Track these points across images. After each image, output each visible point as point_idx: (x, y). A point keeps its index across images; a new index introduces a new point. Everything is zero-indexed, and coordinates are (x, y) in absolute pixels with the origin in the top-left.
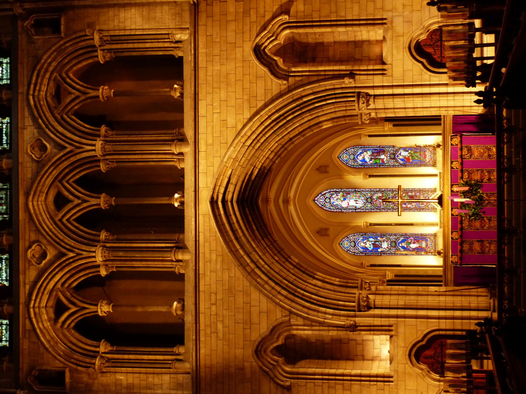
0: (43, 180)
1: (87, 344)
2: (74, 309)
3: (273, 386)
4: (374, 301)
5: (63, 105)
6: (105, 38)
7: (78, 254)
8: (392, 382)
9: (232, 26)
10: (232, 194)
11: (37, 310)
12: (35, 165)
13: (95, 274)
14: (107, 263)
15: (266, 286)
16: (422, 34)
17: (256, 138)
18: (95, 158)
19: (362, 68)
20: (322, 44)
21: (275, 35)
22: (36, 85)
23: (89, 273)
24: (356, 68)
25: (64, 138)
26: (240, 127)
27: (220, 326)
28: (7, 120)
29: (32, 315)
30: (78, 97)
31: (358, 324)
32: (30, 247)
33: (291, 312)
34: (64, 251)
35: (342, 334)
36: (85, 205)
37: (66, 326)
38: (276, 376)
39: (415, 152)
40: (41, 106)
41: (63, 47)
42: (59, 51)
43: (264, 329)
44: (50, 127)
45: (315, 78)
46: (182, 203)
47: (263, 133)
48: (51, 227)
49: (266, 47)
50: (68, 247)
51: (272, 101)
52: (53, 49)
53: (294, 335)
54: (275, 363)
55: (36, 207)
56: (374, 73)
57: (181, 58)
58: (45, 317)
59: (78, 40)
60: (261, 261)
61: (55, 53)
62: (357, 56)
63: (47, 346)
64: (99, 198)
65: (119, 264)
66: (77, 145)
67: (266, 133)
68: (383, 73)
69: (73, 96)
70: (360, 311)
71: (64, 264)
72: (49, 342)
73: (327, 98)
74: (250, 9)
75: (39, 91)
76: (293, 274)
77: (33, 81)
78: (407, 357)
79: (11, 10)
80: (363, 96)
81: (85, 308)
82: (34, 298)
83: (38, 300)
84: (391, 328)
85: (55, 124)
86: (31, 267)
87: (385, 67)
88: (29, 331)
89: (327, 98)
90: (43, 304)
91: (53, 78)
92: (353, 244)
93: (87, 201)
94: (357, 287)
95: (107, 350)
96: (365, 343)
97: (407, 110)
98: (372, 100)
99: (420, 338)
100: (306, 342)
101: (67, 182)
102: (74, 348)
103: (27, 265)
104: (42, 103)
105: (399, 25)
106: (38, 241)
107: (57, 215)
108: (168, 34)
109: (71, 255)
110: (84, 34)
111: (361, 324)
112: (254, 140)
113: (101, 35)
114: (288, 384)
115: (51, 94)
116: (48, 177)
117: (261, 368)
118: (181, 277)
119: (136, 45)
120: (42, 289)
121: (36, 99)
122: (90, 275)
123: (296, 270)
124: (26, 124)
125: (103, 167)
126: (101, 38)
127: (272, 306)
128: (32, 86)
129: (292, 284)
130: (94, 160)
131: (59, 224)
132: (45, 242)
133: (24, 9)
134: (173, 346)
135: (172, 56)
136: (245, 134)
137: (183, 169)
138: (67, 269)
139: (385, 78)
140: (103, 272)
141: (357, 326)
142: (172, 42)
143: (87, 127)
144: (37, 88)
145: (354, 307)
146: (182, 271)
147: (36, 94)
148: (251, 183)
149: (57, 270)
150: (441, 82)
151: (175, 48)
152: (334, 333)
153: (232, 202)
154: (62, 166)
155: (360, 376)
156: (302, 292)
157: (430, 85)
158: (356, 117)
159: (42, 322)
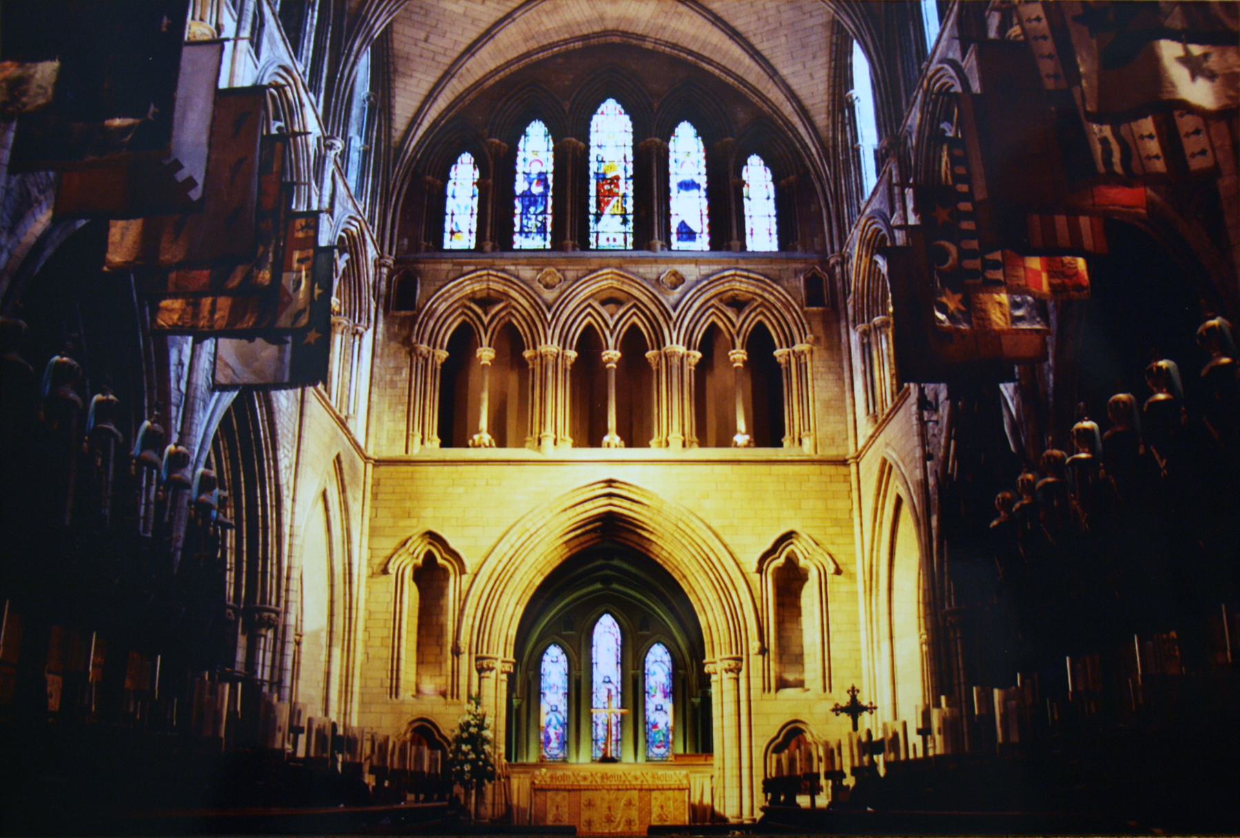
0: (637, 286)
2: (486, 320)
3: (389, 552)
4: (488, 677)
5: (724, 308)
6: (803, 357)
7: (549, 325)
8: (391, 697)
9: (820, 505)
11: (485, 278)
12: (654, 277)
13: (526, 345)
14: (539, 359)
15: (508, 546)
16: (812, 736)
17: (687, 534)
18: (662, 345)
19: (772, 664)
20: (799, 614)
21: (810, 557)
22: (748, 278)
24: (772, 656)
25: (686, 309)
26: (701, 515)
27: (461, 490)
28: (707, 248)
29: (479, 273)
30: (734, 326)
31: (461, 656)
32: (559, 270)
33: (476, 575)
34: (554, 309)
36: (607, 333)
37: (466, 311)
38: (400, 556)
39: (664, 735)
40: (723, 283)
41: (791, 309)
42: (787, 305)
44: (699, 293)
45: (759, 606)
46: (609, 446)
47: (693, 543)
48: (582, 294)
49: (796, 546)
50: (558, 313)
51: (731, 554)
52: (789, 298)
53: (447, 579)
54: (415, 555)
55: (605, 277)
56: (765, 677)
57: (781, 445)
58: (477, 287)
59: (800, 326)
60: (538, 539)
61: (784, 300)
62: (784, 657)
63: (443, 290)
64: (615, 349)
65: (538, 370)
66: (678, 324)
67: (693, 546)
68: (766, 688)
69: (734, 319)
70: (477, 659)
71: (537, 308)
72: (448, 291)
73: (736, 620)
74: (841, 527)
75: (740, 282)
76: (521, 579)
77: (751, 275)
78: (420, 716)
79: (833, 251)
80: (737, 665)
81: (486, 335)
82: (500, 274)
83: (497, 279)
84: (455, 697)
85: (701, 300)
86: (535, 272)
87: (773, 690)
88: (462, 270)
89: (736, 620)
90: (492, 285)
91: (755, 297)
92: (555, 659)
93: (611, 334)
94: (505, 656)
95: (436, 358)
96: (438, 665)
97: (720, 719)
98: (732, 675)
99: (442, 732)
100: (441, 593)
101: (635, 314)
102: (441, 321)
103: (538, 267)
104: (727, 285)
106: (565, 280)
107: (596, 299)
108: (809, 430)
109: (549, 317)
110: (808, 332)
111: (460, 661)
112: (684, 531)
113: (806, 352)
114: (390, 571)
115: (737, 295)
116: (640, 291)
117: (410, 538)
119: (795, 392)
120: (509, 284)
121: (731, 278)
122: (525, 339)
123: (527, 582)
124: (702, 267)
125: (650, 354)
126: (802, 352)
127: (484, 552)
128: (745, 274)
129: (511, 577)
130: (659, 342)
132: (565, 286)
133: (834, 267)
134: (439, 435)
135: (783, 435)
136: (691, 521)
137: (649, 446)
138: (532, 312)
139: (760, 691)
141: (458, 656)
142: (800, 434)
143: (698, 336)
144: (744, 280)
145: (482, 652)
146: (528, 444)
147: (737, 278)
148: (632, 528)
149: (532, 301)
150: (754, 760)
151: (794, 438)
153: (611, 505)
154: (652, 307)
155: (398, 659)
156: (500, 589)
157: (751, 747)
158: (711, 656)
159: (472, 284)
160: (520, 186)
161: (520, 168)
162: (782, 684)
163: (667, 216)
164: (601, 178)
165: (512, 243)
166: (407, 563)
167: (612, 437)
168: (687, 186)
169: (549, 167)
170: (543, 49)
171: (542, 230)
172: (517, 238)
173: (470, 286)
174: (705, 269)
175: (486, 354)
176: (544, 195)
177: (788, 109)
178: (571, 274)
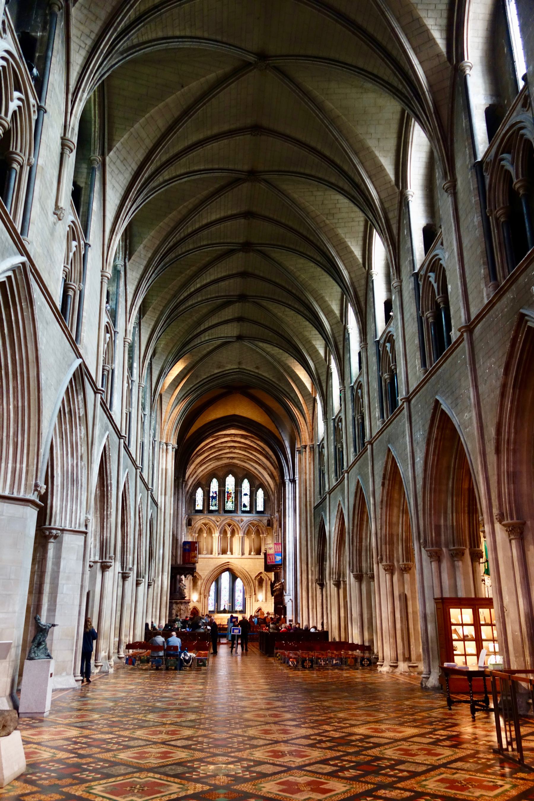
1: (197, 531)
10: (230, 567)
43: (200, 574)
57: (260, 554)
105: (265, 605)
118: (212, 554)
125: (236, 535)
131: (225, 525)
140: (213, 535)
143: (246, 532)
160: (211, 495)
161: (211, 490)
163: (241, 502)
164: (228, 492)
165: (209, 508)
167: (229, 553)
168: (246, 495)
169: (217, 490)
170: (217, 466)
171: (216, 505)
172: (211, 507)
173: (203, 521)
174: (248, 518)
176: (216, 497)
177: (266, 483)
178: (222, 519)
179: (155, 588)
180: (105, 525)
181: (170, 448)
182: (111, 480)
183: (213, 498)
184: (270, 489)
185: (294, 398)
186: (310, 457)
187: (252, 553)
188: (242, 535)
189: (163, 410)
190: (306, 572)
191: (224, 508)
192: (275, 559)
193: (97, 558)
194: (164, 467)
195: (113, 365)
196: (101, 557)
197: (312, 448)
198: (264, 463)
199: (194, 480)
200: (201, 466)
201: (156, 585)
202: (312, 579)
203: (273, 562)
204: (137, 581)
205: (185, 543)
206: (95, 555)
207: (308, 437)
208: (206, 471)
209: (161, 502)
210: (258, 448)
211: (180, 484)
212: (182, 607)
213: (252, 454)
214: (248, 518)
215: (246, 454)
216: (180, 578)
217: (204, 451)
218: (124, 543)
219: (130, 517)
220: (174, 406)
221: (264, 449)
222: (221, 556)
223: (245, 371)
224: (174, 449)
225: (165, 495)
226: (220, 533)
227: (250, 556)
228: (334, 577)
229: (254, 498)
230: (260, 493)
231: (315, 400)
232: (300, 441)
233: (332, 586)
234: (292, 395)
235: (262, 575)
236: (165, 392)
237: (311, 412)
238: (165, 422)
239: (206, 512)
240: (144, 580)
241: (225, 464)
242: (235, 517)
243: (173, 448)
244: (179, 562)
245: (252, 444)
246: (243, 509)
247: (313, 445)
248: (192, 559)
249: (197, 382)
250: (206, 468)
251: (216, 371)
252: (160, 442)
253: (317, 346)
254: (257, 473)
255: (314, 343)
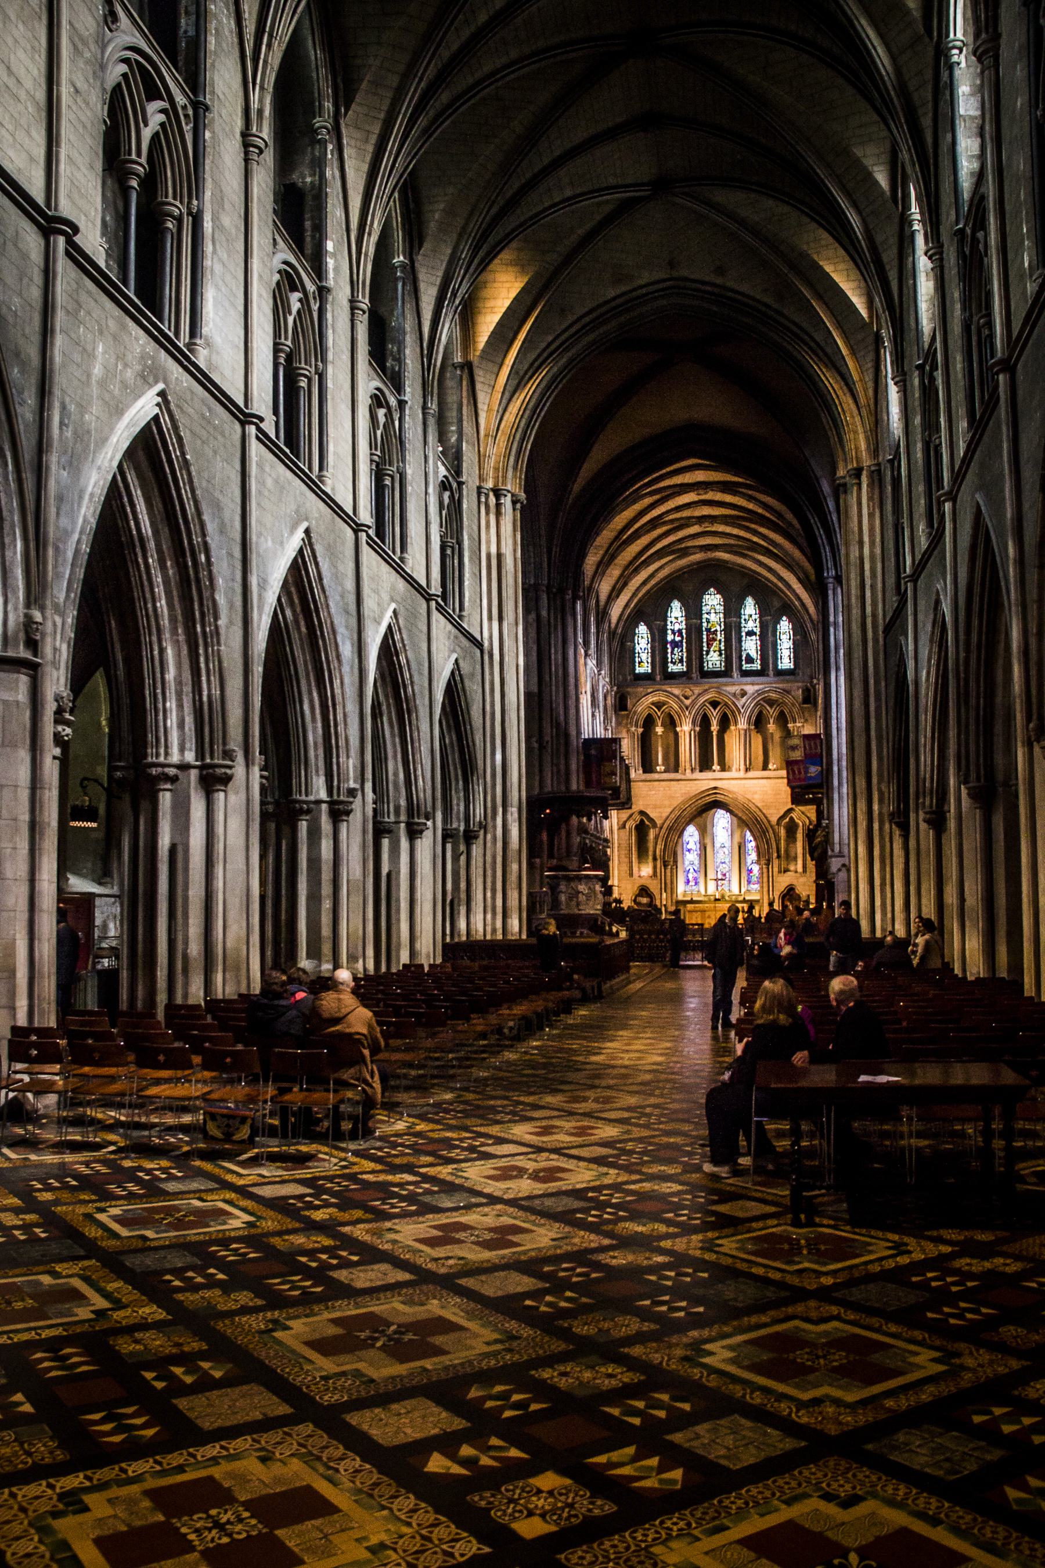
1: (641, 722)
10: (719, 798)
23: (678, 721)
35: (651, 853)
43: (652, 815)
100: (646, 834)
105: (802, 880)
125: (732, 728)
130: (736, 724)
131: (703, 704)
143: (753, 718)
152: (651, 849)
160: (670, 638)
162: (786, 871)
164: (708, 630)
166: (632, 824)
167: (716, 767)
168: (750, 633)
171: (681, 661)
173: (652, 699)
174: (757, 687)
175: (659, 730)
178: (696, 692)
179: (489, 845)
180: (203, 665)
181: (507, 501)
182: (204, 535)
183: (675, 644)
184: (806, 617)
185: (823, 344)
186: (870, 499)
187: (770, 766)
188: (745, 727)
189: (480, 406)
190: (864, 796)
191: (701, 666)
192: (806, 772)
193: (190, 757)
194: (494, 550)
195: (195, 202)
196: (200, 754)
197: (877, 477)
198: (786, 553)
199: (627, 606)
200: (637, 571)
201: (489, 837)
202: (880, 814)
203: (800, 780)
204: (409, 825)
205: (589, 743)
206: (182, 750)
207: (863, 446)
208: (653, 582)
209: (491, 637)
210: (768, 515)
211: (568, 605)
212: (582, 888)
213: (755, 533)
214: (757, 687)
215: (742, 533)
216: (580, 822)
217: (637, 530)
218: (329, 726)
219: (338, 656)
220: (507, 395)
221: (779, 515)
222: (698, 775)
223: (688, 284)
224: (518, 506)
225: (501, 619)
226: (694, 723)
227: (765, 773)
228: (927, 803)
229: (771, 639)
230: (785, 626)
231: (878, 339)
232: (845, 460)
233: (923, 826)
234: (819, 337)
235: (793, 815)
236: (481, 357)
237: (869, 377)
238: (487, 436)
239: (658, 678)
240: (429, 823)
241: (699, 563)
242: (726, 685)
243: (514, 503)
244: (574, 787)
245: (751, 506)
246: (746, 666)
247: (879, 465)
248: (607, 780)
249: (563, 327)
250: (652, 576)
251: (611, 293)
252: (479, 488)
253: (865, 161)
254: (775, 580)
255: (858, 152)
